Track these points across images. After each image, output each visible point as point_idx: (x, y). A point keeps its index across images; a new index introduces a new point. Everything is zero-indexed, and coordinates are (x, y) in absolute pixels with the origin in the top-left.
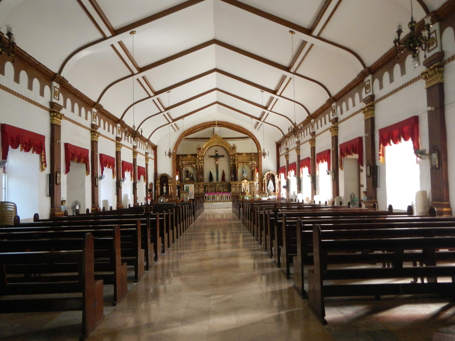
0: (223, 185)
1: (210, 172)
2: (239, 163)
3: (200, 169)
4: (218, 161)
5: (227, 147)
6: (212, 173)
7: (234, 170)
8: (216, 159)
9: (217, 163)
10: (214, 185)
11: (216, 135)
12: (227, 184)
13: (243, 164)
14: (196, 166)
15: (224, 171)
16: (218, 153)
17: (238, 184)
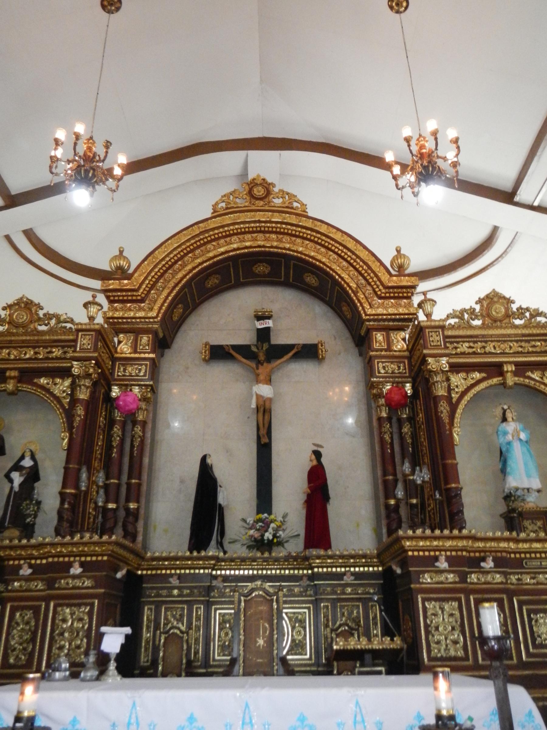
0: (313, 577)
1: (204, 458)
2: (455, 368)
3: (117, 430)
4: (269, 381)
5: (344, 263)
6: (218, 473)
7: (409, 441)
8: (259, 363)
9: (265, 390)
10: (226, 579)
11: (253, 184)
12: (357, 576)
13: (495, 381)
14: (73, 386)
15: (317, 454)
16: (269, 323)
17: (489, 564)
